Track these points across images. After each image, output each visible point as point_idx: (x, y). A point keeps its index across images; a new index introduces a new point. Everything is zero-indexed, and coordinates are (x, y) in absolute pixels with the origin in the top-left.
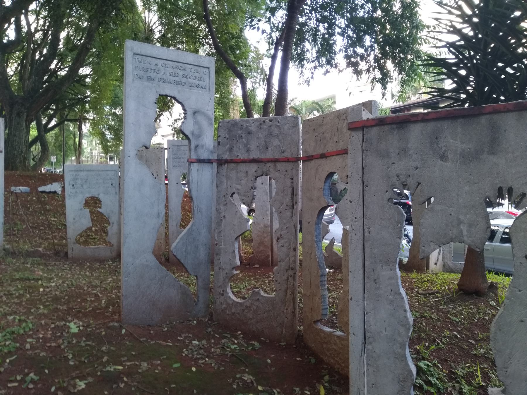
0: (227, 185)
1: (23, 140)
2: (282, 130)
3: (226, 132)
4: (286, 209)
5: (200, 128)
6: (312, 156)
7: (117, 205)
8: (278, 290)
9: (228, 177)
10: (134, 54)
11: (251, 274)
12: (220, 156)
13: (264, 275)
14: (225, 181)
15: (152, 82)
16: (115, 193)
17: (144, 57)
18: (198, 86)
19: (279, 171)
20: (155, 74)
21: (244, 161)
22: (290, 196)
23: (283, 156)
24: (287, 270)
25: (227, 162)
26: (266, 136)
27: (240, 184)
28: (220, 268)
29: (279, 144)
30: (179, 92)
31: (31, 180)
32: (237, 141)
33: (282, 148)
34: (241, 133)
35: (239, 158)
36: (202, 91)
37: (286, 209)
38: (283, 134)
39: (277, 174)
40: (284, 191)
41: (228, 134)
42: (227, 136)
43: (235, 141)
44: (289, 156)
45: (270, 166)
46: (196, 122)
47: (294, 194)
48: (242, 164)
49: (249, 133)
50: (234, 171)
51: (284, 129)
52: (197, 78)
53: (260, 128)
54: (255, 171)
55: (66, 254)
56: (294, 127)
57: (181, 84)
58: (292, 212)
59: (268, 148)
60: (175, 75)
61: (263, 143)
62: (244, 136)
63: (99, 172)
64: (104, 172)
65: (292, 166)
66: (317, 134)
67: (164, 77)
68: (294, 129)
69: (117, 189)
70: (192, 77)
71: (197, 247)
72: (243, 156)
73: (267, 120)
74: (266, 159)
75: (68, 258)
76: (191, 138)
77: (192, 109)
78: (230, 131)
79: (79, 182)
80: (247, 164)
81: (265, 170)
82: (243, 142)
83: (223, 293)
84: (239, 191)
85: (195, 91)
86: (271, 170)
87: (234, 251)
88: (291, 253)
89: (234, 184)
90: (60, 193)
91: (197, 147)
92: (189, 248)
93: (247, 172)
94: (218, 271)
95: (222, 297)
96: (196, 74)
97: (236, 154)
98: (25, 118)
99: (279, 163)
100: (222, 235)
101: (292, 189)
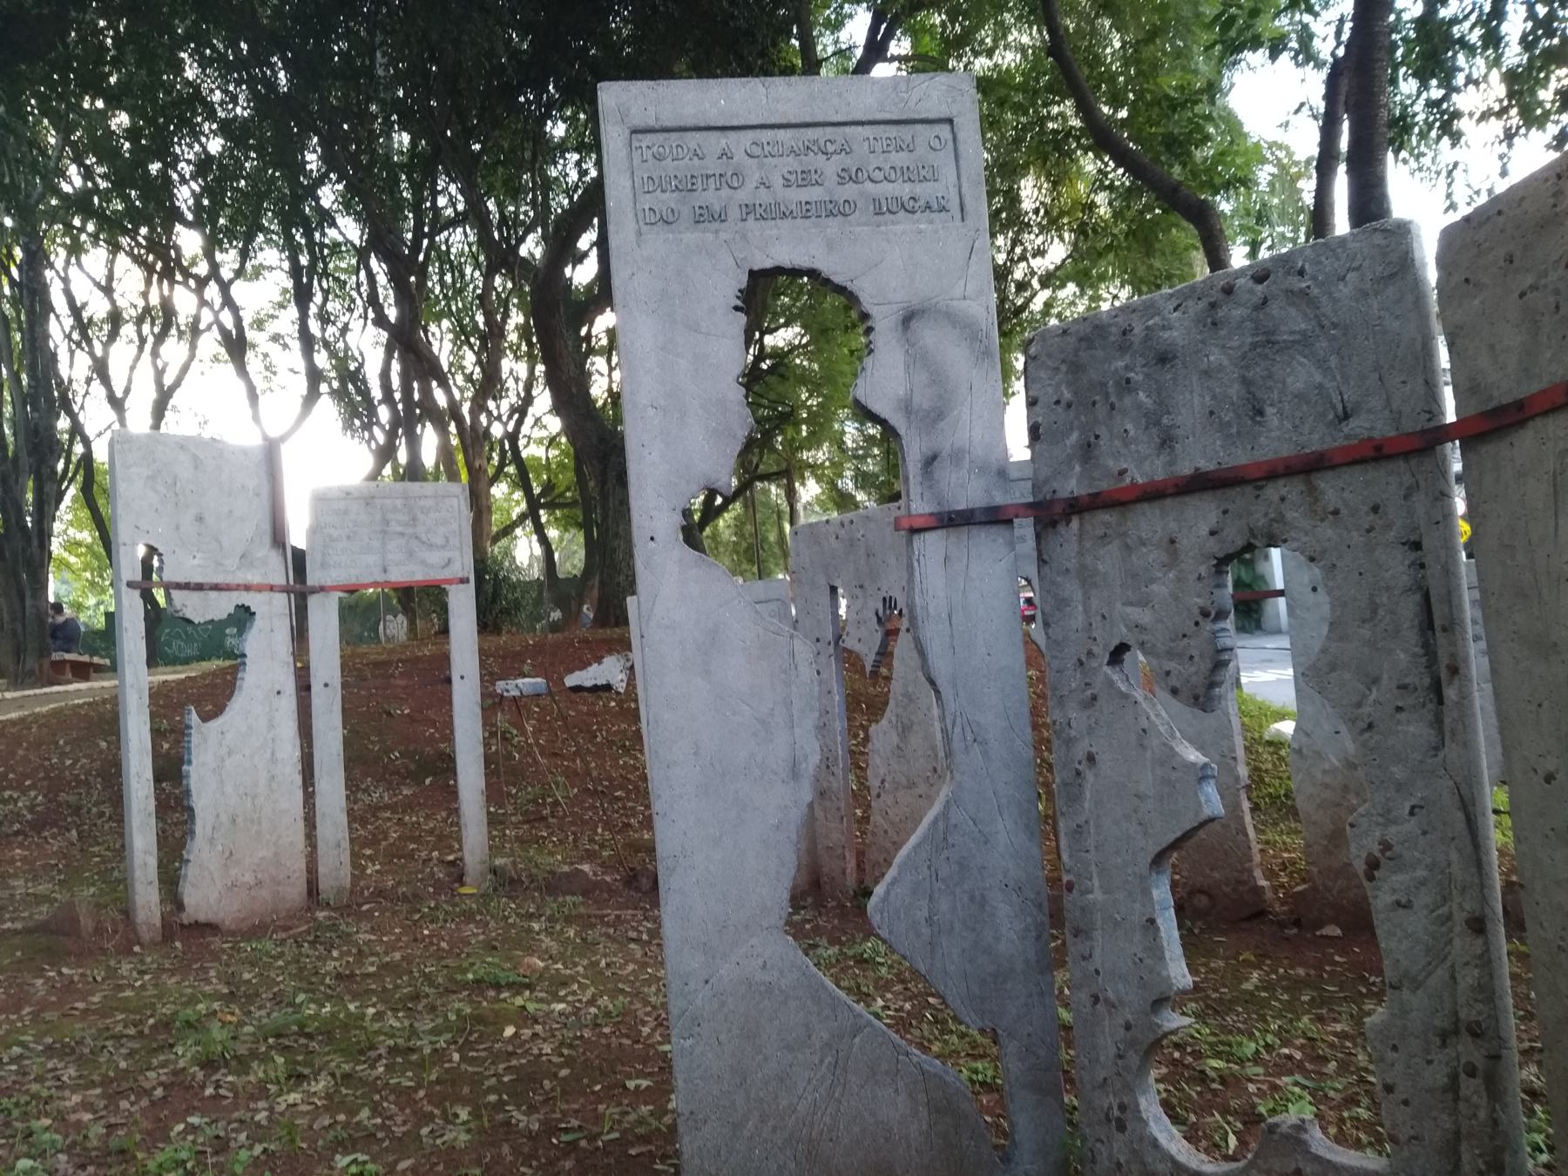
0: (1086, 611)
2: (1326, 308)
3: (1060, 376)
4: (1399, 709)
5: (938, 379)
6: (1519, 405)
8: (1402, 1138)
9: (1087, 578)
10: (635, 131)
11: (1301, 971)
12: (1046, 489)
13: (1364, 980)
14: (1078, 595)
15: (716, 225)
17: (674, 136)
18: (906, 207)
19: (1336, 512)
20: (725, 192)
21: (1153, 494)
22: (1411, 636)
23: (1347, 437)
24: (1445, 1037)
25: (1076, 507)
26: (1244, 357)
27: (1144, 603)
28: (1096, 999)
29: (1318, 378)
30: (830, 246)
32: (1113, 407)
33: (1336, 400)
34: (1127, 368)
35: (1128, 481)
36: (931, 222)
37: (1399, 709)
38: (1335, 326)
39: (1327, 531)
40: (1375, 612)
41: (1069, 384)
42: (1067, 395)
43: (1101, 410)
44: (1382, 428)
45: (1283, 499)
46: (918, 359)
47: (1438, 623)
48: (1146, 506)
49: (1164, 358)
50: (1114, 547)
51: (1335, 301)
52: (907, 175)
53: (1214, 324)
54: (1212, 533)
56: (1392, 276)
57: (837, 210)
58: (1438, 722)
59: (1261, 413)
60: (806, 178)
61: (1235, 391)
62: (1140, 377)
65: (1407, 479)
66: (1529, 280)
67: (764, 196)
68: (1391, 292)
70: (878, 175)
71: (980, 902)
72: (1145, 468)
73: (1241, 281)
74: (1258, 465)
76: (902, 431)
77: (895, 307)
78: (1076, 368)
80: (1169, 502)
81: (1262, 521)
82: (1139, 406)
83: (1124, 1119)
84: (1145, 638)
85: (899, 228)
86: (1290, 515)
87: (1152, 921)
88: (1457, 942)
89: (1118, 605)
90: (621, 688)
91: (930, 461)
92: (944, 906)
93: (1172, 541)
94: (1089, 1009)
95: (1119, 1136)
96: (901, 159)
97: (1112, 465)
99: (1330, 474)
100: (1090, 843)
101: (1418, 597)
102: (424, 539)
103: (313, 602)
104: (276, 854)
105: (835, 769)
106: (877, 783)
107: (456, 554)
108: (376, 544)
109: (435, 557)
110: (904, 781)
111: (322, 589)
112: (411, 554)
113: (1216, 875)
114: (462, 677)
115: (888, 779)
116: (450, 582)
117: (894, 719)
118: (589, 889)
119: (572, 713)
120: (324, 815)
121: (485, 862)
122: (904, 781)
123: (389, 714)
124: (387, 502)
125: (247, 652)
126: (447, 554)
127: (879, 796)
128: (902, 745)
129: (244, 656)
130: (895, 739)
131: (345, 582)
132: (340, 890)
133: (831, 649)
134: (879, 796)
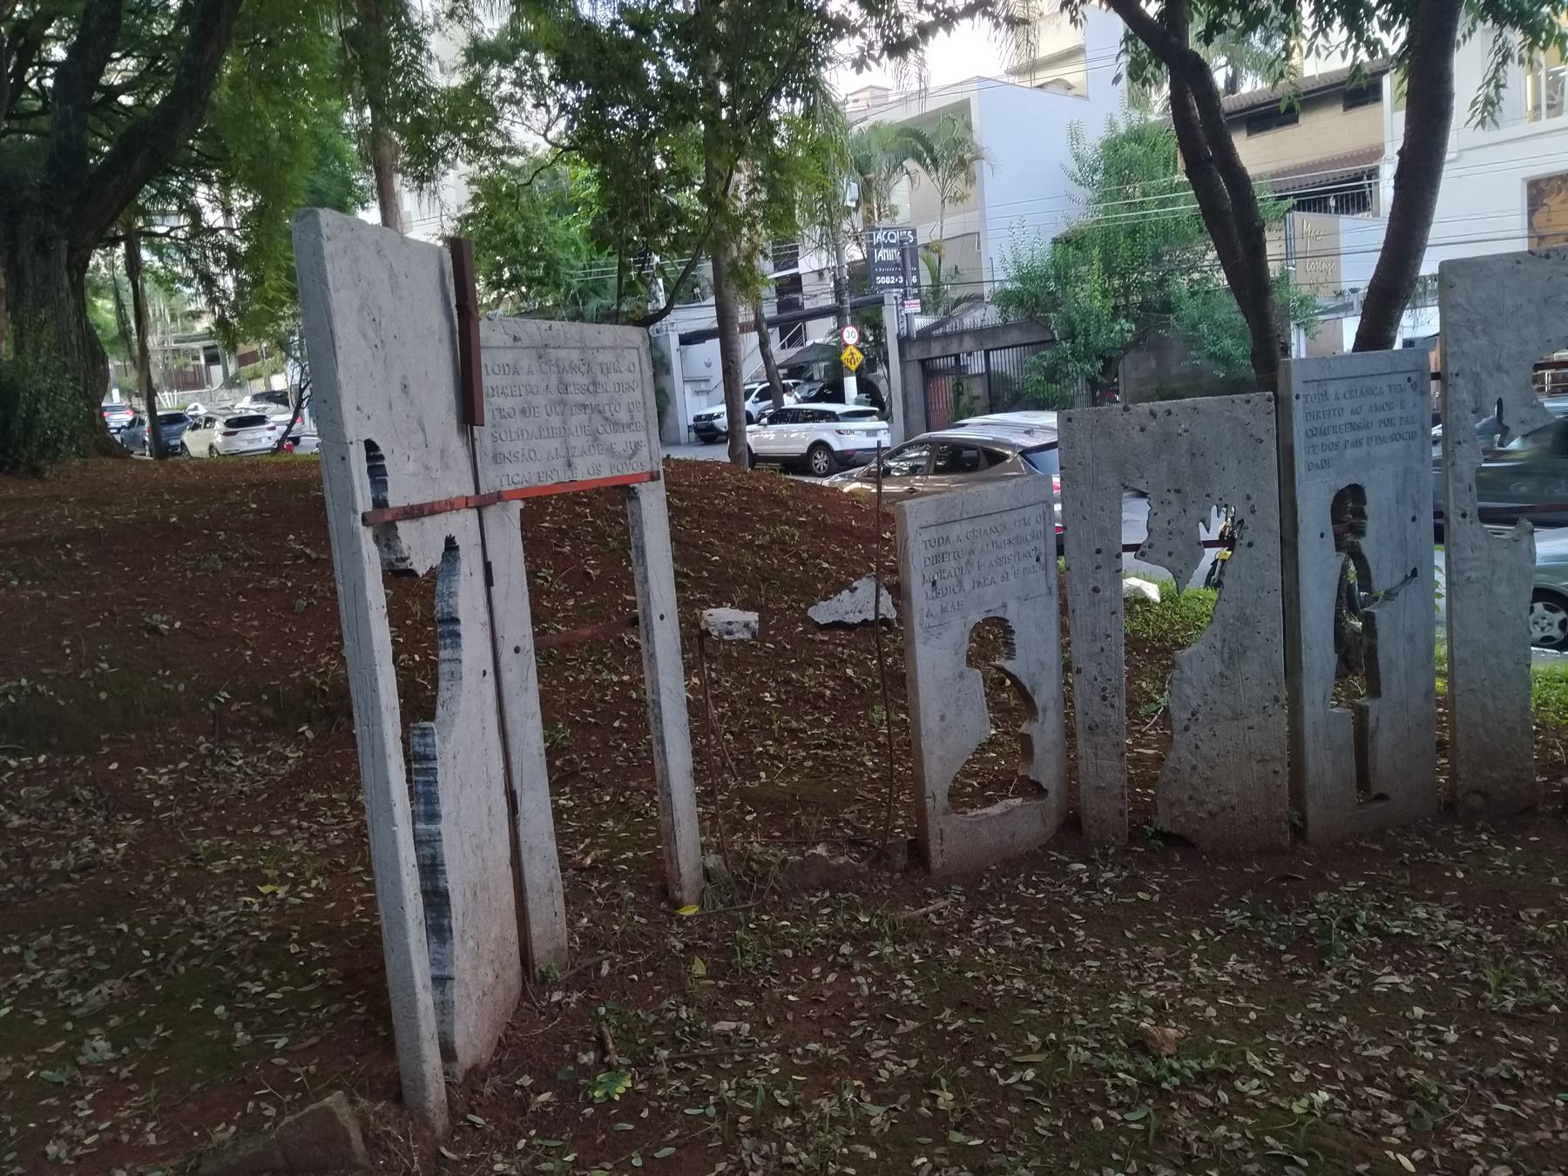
1: (73, 337)
7: (1053, 632)
16: (1044, 589)
55: (918, 851)
63: (1004, 515)
75: (928, 872)
79: (950, 565)
98: (64, 257)
102: (608, 414)
105: (1116, 701)
107: (640, 436)
109: (621, 441)
110: (1227, 712)
112: (595, 436)
113: (1495, 775)
115: (1202, 710)
116: (639, 478)
117: (1218, 645)
118: (834, 881)
120: (531, 849)
122: (1227, 712)
124: (562, 353)
125: (462, 616)
127: (1187, 729)
128: (1228, 673)
129: (456, 621)
130: (1218, 666)
131: (525, 485)
134: (1187, 729)
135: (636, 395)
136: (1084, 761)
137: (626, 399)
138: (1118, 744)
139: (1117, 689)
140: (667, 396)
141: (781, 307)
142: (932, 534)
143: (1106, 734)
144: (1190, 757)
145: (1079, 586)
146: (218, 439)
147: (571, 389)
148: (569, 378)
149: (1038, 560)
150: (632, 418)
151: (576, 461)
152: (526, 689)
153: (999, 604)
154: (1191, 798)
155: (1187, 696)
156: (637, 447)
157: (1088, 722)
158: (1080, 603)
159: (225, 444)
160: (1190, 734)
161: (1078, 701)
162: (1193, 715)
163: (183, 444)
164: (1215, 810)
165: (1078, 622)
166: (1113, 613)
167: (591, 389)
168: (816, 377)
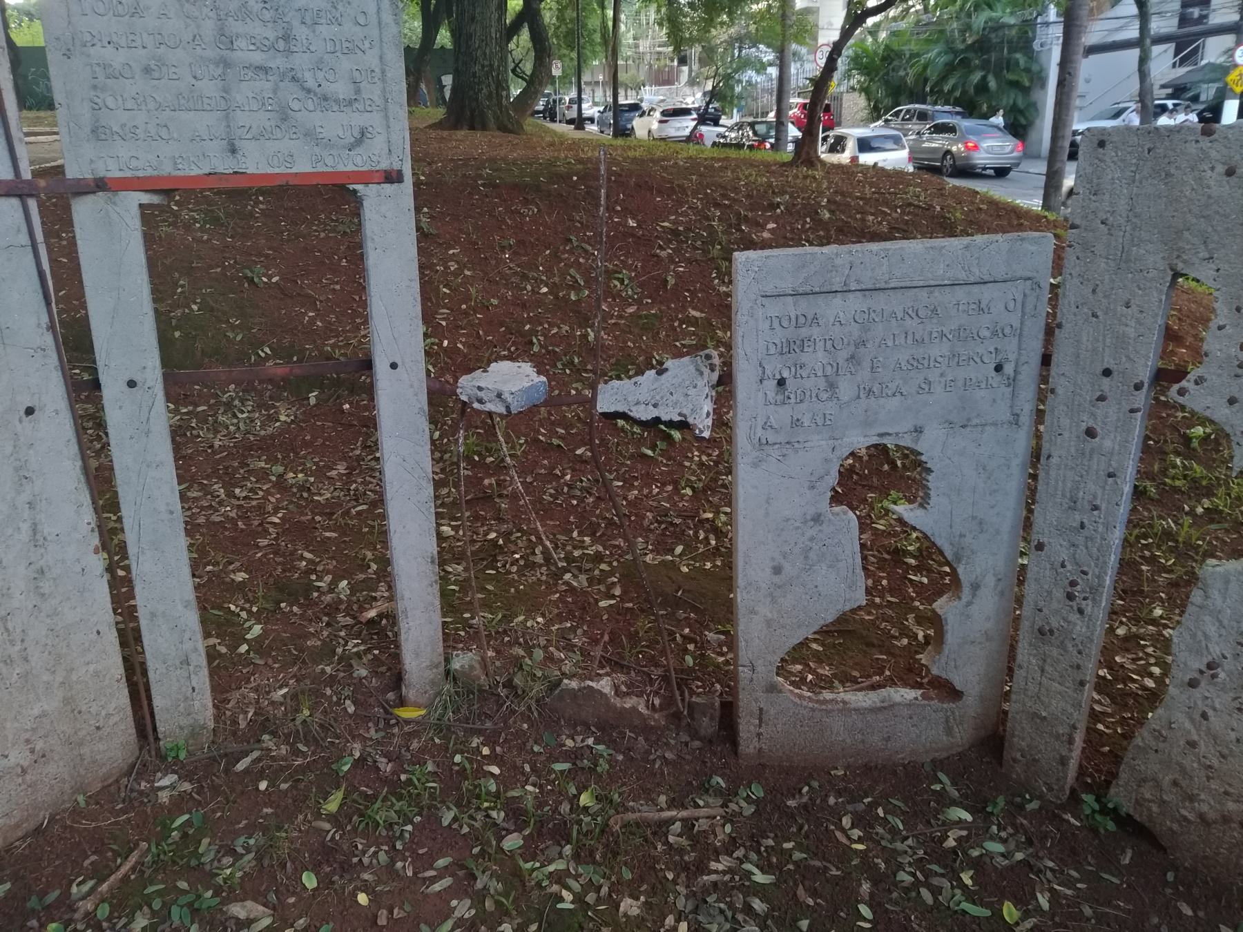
1: (493, 30)
7: (1013, 484)
16: (1007, 416)
31: (526, 202)
64: (960, 292)
69: (1027, 394)
79: (816, 358)
90: (704, 425)
102: (311, 83)
103: (84, 211)
104: (67, 701)
105: (1088, 607)
106: (1198, 663)
108: (209, 88)
109: (335, 125)
111: (100, 185)
112: (284, 115)
114: (394, 366)
115: (1228, 664)
116: (366, 178)
119: (495, 302)
121: (437, 666)
123: (251, 281)
126: (358, 120)
127: (1193, 684)
131: (149, 172)
132: (195, 731)
133: (1141, 399)
134: (1193, 684)
135: (371, 59)
136: (1023, 672)
137: (346, 64)
138: (1078, 667)
139: (1094, 591)
140: (1037, 110)
141: (1184, 20)
142: (790, 307)
143: (1062, 646)
144: (1188, 725)
145: (1065, 422)
146: (655, 126)
147: (241, 43)
148: (235, 27)
149: (998, 368)
150: (358, 91)
151: (246, 146)
152: (148, 433)
153: (909, 426)
154: (1175, 783)
155: (1205, 635)
156: (362, 136)
157: (1039, 623)
158: (1062, 447)
159: (659, 129)
160: (1197, 693)
161: (1030, 589)
162: (1210, 666)
163: (633, 128)
164: (1212, 815)
165: (1053, 473)
166: (1110, 475)
167: (281, 45)
168: (1203, 98)
